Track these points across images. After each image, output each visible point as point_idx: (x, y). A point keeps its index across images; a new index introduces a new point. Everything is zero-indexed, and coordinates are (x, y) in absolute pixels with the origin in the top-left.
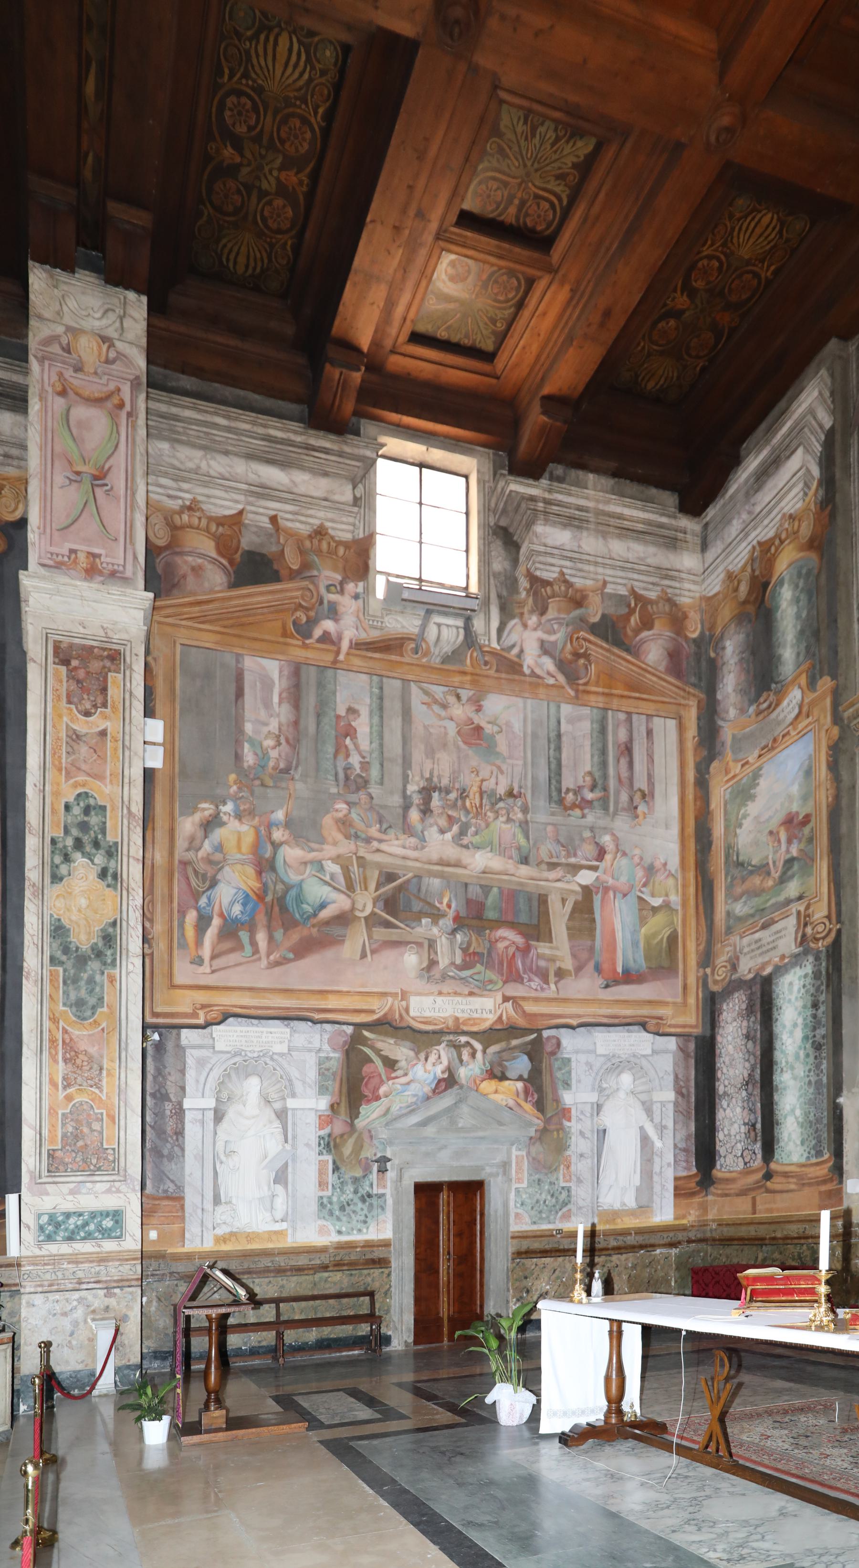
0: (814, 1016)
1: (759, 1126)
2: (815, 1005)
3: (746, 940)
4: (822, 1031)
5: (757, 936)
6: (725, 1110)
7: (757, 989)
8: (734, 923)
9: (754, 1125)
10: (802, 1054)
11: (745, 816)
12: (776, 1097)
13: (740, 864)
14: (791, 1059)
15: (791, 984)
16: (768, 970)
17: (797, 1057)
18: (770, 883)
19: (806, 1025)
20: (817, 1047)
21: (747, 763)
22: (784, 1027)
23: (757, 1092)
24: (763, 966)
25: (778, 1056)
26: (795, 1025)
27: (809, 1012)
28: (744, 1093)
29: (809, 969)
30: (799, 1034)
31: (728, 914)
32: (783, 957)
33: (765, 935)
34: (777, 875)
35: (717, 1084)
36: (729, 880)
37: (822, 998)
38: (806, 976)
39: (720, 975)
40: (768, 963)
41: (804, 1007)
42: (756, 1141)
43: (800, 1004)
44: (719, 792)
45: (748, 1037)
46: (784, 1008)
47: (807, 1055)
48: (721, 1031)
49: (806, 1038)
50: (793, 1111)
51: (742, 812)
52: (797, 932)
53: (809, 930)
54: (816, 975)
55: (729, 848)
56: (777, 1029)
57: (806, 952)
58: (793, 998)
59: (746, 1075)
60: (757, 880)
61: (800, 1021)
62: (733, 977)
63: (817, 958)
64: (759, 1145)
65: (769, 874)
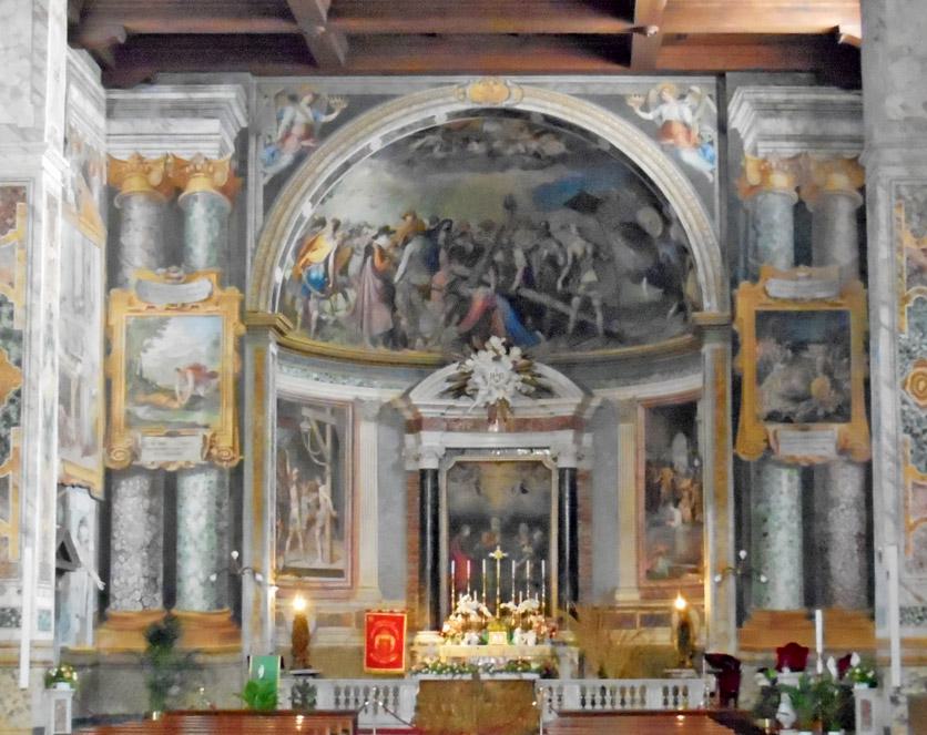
0: (218, 512)
1: (160, 580)
2: (219, 505)
3: (148, 439)
4: (224, 524)
5: (163, 439)
6: (122, 563)
7: (161, 480)
8: (131, 422)
9: (155, 580)
10: (206, 535)
11: (149, 346)
12: (179, 562)
14: (195, 537)
15: (196, 485)
16: (172, 468)
17: (201, 537)
18: (176, 405)
19: (209, 516)
20: (220, 533)
21: (153, 307)
22: (189, 512)
23: (160, 554)
24: (169, 463)
25: (182, 532)
26: (199, 514)
27: (214, 508)
28: (145, 554)
29: (213, 477)
30: (203, 521)
31: (128, 413)
32: (188, 463)
33: (171, 442)
34: (184, 402)
35: (112, 542)
36: (130, 386)
37: (226, 501)
38: (211, 482)
39: (120, 457)
40: (174, 462)
41: (209, 503)
42: (155, 592)
43: (205, 500)
44: (121, 317)
45: (150, 512)
46: (189, 498)
47: (210, 537)
48: (119, 501)
49: (209, 526)
50: (195, 574)
51: (146, 342)
52: (203, 449)
54: (220, 484)
55: (130, 365)
56: (181, 512)
57: (212, 466)
58: (198, 494)
59: (148, 541)
60: (163, 399)
61: (205, 512)
62: (135, 463)
63: (221, 471)
64: (159, 596)
65: (174, 398)
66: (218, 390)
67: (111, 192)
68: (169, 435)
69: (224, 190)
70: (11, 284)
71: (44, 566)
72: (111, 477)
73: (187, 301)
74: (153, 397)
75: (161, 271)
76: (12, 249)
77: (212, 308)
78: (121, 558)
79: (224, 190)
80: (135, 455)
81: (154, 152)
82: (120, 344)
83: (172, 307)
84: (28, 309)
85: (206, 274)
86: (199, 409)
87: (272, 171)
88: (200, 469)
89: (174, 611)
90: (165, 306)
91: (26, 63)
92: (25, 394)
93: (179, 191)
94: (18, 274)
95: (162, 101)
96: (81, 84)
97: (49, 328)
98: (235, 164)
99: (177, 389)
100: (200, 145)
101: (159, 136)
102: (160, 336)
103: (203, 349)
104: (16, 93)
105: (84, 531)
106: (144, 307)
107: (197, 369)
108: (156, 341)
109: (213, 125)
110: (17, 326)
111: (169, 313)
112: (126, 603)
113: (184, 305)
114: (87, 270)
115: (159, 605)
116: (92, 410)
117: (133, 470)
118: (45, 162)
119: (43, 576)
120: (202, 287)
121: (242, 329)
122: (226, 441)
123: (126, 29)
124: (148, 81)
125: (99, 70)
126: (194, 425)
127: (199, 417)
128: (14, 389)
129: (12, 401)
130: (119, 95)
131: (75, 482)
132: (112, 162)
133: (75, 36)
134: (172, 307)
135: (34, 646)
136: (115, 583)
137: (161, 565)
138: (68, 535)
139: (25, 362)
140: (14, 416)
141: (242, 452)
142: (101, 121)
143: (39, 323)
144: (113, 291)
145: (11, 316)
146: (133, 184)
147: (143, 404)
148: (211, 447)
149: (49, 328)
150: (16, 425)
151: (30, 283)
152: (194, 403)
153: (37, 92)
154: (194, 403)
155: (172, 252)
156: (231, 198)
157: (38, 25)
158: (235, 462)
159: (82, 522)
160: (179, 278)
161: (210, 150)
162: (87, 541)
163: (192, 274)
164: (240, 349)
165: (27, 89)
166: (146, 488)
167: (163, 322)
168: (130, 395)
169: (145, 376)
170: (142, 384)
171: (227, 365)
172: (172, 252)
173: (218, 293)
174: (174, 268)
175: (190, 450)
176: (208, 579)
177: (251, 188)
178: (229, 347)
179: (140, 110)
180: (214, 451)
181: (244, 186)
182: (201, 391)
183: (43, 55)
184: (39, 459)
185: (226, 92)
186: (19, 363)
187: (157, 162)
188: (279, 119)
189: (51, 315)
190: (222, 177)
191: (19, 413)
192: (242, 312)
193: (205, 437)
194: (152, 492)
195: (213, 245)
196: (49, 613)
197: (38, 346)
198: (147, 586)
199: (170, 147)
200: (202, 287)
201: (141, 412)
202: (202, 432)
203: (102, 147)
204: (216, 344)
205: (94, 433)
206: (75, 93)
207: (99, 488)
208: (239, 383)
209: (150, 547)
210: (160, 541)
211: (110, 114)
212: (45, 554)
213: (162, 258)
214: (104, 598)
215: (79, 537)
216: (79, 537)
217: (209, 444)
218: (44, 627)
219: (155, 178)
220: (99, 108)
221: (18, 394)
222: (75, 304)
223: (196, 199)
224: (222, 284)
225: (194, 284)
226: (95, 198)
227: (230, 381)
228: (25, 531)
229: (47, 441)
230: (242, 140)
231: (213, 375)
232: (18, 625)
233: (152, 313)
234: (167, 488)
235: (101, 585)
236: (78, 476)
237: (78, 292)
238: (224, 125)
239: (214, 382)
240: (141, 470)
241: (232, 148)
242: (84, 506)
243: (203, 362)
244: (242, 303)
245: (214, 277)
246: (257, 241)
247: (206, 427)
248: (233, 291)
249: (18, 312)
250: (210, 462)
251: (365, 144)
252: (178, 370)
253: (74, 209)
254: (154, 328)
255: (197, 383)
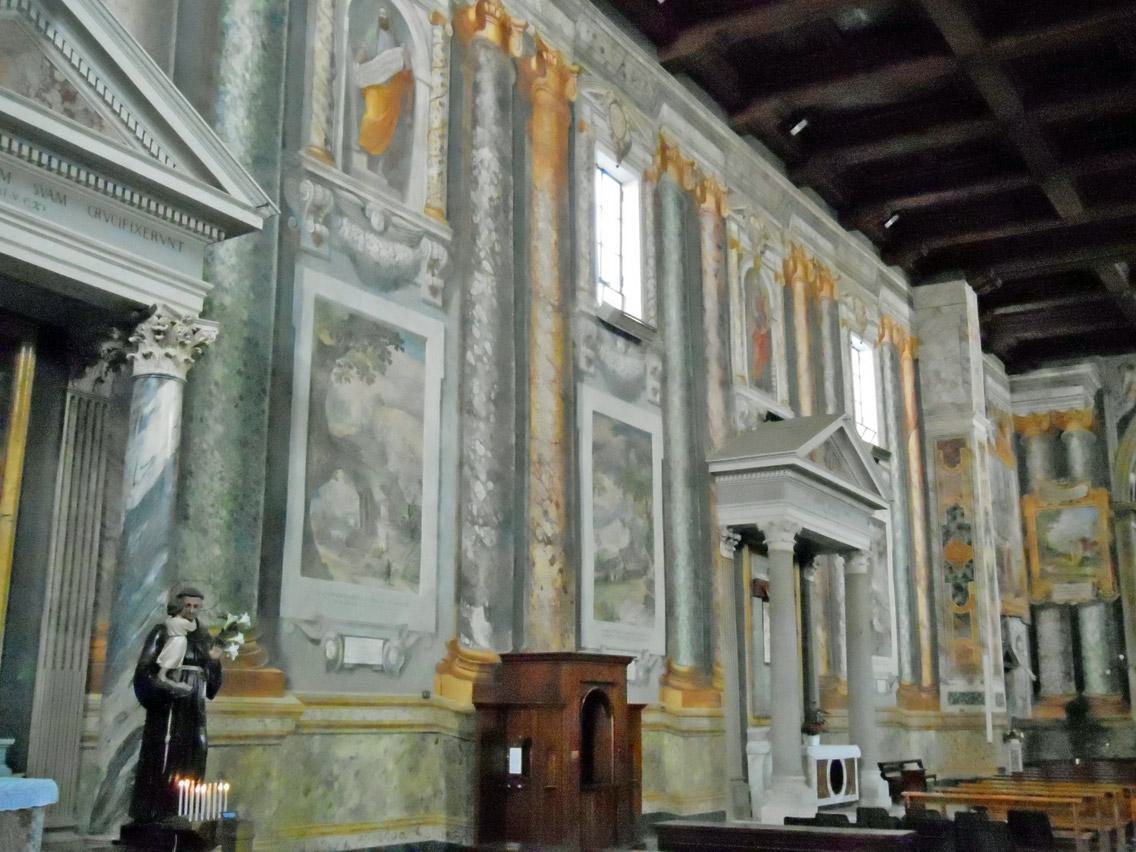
1: (1073, 673)
2: (1107, 625)
8: (1044, 575)
11: (1052, 528)
13: (1049, 549)
16: (1074, 603)
20: (1109, 643)
29: (1102, 607)
30: (1097, 636)
31: (1042, 570)
33: (1073, 587)
35: (1039, 651)
39: (1038, 597)
44: (1031, 511)
45: (1062, 631)
49: (1102, 639)
51: (1050, 525)
53: (1101, 591)
54: (1107, 612)
60: (1064, 560)
63: (1107, 605)
64: (1073, 684)
65: (1070, 559)
66: (1098, 553)
67: (1018, 436)
68: (1070, 583)
69: (1091, 428)
70: (961, 496)
71: (996, 666)
72: (1034, 611)
73: (1072, 498)
74: (1057, 559)
75: (1054, 481)
76: (960, 475)
77: (1090, 502)
78: (1046, 661)
79: (1091, 428)
80: (1048, 595)
81: (1043, 409)
82: (1032, 528)
83: (1063, 503)
84: (973, 512)
85: (1082, 482)
86: (1087, 566)
87: (1121, 414)
88: (1093, 603)
89: (1084, 694)
90: (1059, 502)
91: (958, 366)
92: (976, 561)
93: (1062, 432)
94: (964, 490)
95: (1045, 378)
96: (993, 375)
97: (987, 522)
98: (1096, 412)
99: (1072, 553)
100: (1072, 403)
101: (1045, 400)
102: (1058, 522)
103: (1087, 527)
104: (954, 384)
105: (1020, 644)
106: (1045, 504)
107: (1084, 541)
108: (1055, 525)
109: (1079, 390)
110: (966, 522)
111: (1061, 507)
112: (1051, 688)
113: (1071, 501)
114: (1007, 485)
115: (1073, 690)
116: (1017, 568)
117: (1048, 605)
118: (975, 422)
119: (997, 672)
120: (1082, 489)
121: (1112, 513)
122: (1108, 583)
123: (1017, 338)
124: (1036, 367)
125: (1003, 366)
126: (1086, 576)
127: (1089, 570)
128: (968, 560)
129: (968, 566)
130: (1017, 378)
131: (1012, 614)
132: (1017, 419)
133: (987, 347)
134: (1063, 503)
135: (995, 716)
136: (1044, 677)
137: (1072, 665)
138: (1010, 646)
139: (974, 541)
140: (969, 575)
141: (1119, 592)
142: (1007, 395)
143: (980, 519)
144: (1026, 496)
145: (963, 515)
146: (1031, 431)
147: (1051, 564)
148: (1098, 589)
149: (987, 522)
150: (971, 580)
151: (972, 494)
152: (1084, 561)
153: (967, 383)
154: (1084, 561)
155: (1060, 468)
156: (1096, 433)
157: (963, 343)
158: (1115, 599)
159: (1018, 639)
160: (1066, 485)
161: (1079, 405)
162: (1023, 651)
163: (1074, 482)
164: (1112, 524)
165: (960, 380)
166: (1058, 616)
167: (1058, 513)
168: (1042, 557)
169: (1051, 546)
170: (1047, 551)
171: (1104, 537)
172: (1060, 468)
173: (1092, 492)
174: (1062, 479)
175: (1083, 592)
176: (1104, 673)
177: (1108, 425)
178: (1104, 525)
179: (1031, 386)
180: (1101, 591)
181: (1103, 424)
182: (1088, 554)
183: (968, 360)
184: (987, 600)
185: (1085, 368)
186: (970, 543)
187: (1045, 416)
188: (1123, 381)
189: (986, 513)
190: (1089, 419)
191: (973, 572)
192: (1110, 502)
193: (1094, 584)
194: (1062, 618)
195: (1086, 464)
196: (1001, 695)
197: (981, 532)
198: (1064, 678)
199: (1053, 406)
200: (1082, 489)
201: (1050, 569)
202: (1091, 580)
203: (1010, 411)
204: (1094, 524)
205: (1021, 581)
206: (990, 380)
207: (1027, 616)
208: (1113, 550)
209: (1064, 653)
210: (1070, 649)
211: (1012, 390)
212: (996, 659)
213: (1054, 473)
214: (1037, 686)
215: (1017, 648)
216: (1017, 648)
217: (1097, 587)
218: (999, 704)
219: (1045, 425)
220: (1004, 386)
221: (971, 561)
222: (1001, 506)
223: (1072, 436)
224: (1095, 485)
225: (1076, 488)
226: (1008, 440)
227: (1107, 549)
228: (982, 645)
229: (992, 591)
230: (1099, 397)
231: (1095, 543)
232: (983, 702)
233: (1052, 507)
234: (1071, 617)
235: (1034, 677)
236: (1012, 610)
237: (1003, 497)
238: (1086, 388)
239: (1097, 548)
240: (1054, 605)
241: (1093, 402)
242: (1018, 629)
243: (1087, 536)
244: (1110, 497)
245: (1089, 483)
246: (1116, 458)
247: (1094, 576)
248: (1103, 491)
249: (966, 513)
250: (1098, 599)
251: (977, 443)
252: (1071, 542)
253: (995, 448)
254: (1053, 516)
255: (1085, 549)
